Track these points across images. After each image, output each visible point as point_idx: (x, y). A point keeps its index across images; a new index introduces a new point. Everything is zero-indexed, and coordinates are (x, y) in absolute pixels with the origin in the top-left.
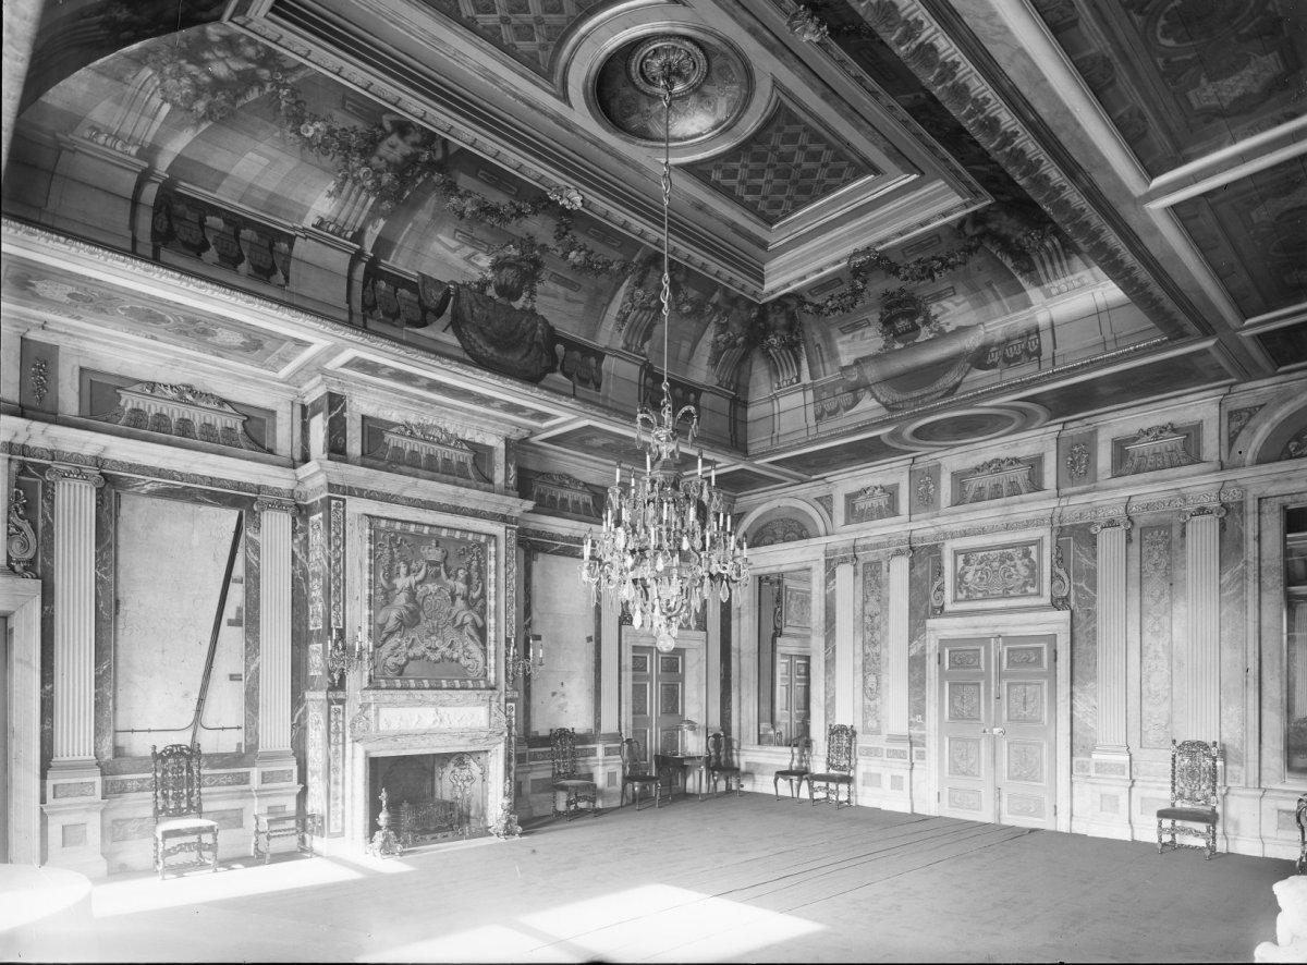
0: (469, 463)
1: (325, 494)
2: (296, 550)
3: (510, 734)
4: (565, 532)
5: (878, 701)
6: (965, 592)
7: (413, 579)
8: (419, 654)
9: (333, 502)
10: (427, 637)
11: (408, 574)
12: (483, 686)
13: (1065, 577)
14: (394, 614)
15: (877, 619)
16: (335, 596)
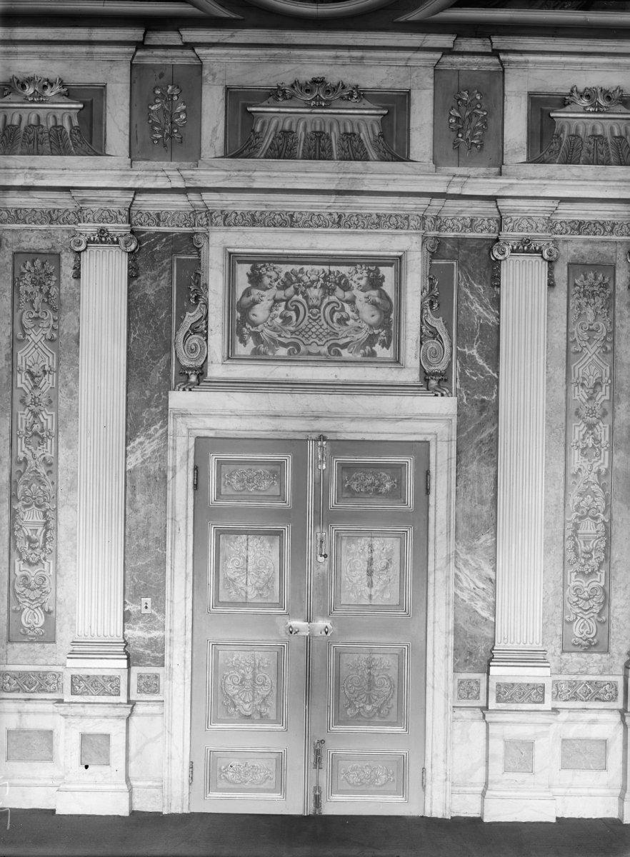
5: (48, 568)
13: (444, 336)
15: (47, 382)
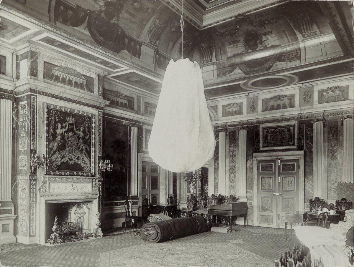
0: (85, 84)
1: (29, 93)
2: (14, 116)
3: (100, 195)
4: (118, 115)
6: (267, 143)
7: (63, 130)
9: (32, 97)
10: (68, 154)
11: (61, 128)
12: (90, 175)
13: (302, 139)
14: (56, 144)
16: (33, 136)
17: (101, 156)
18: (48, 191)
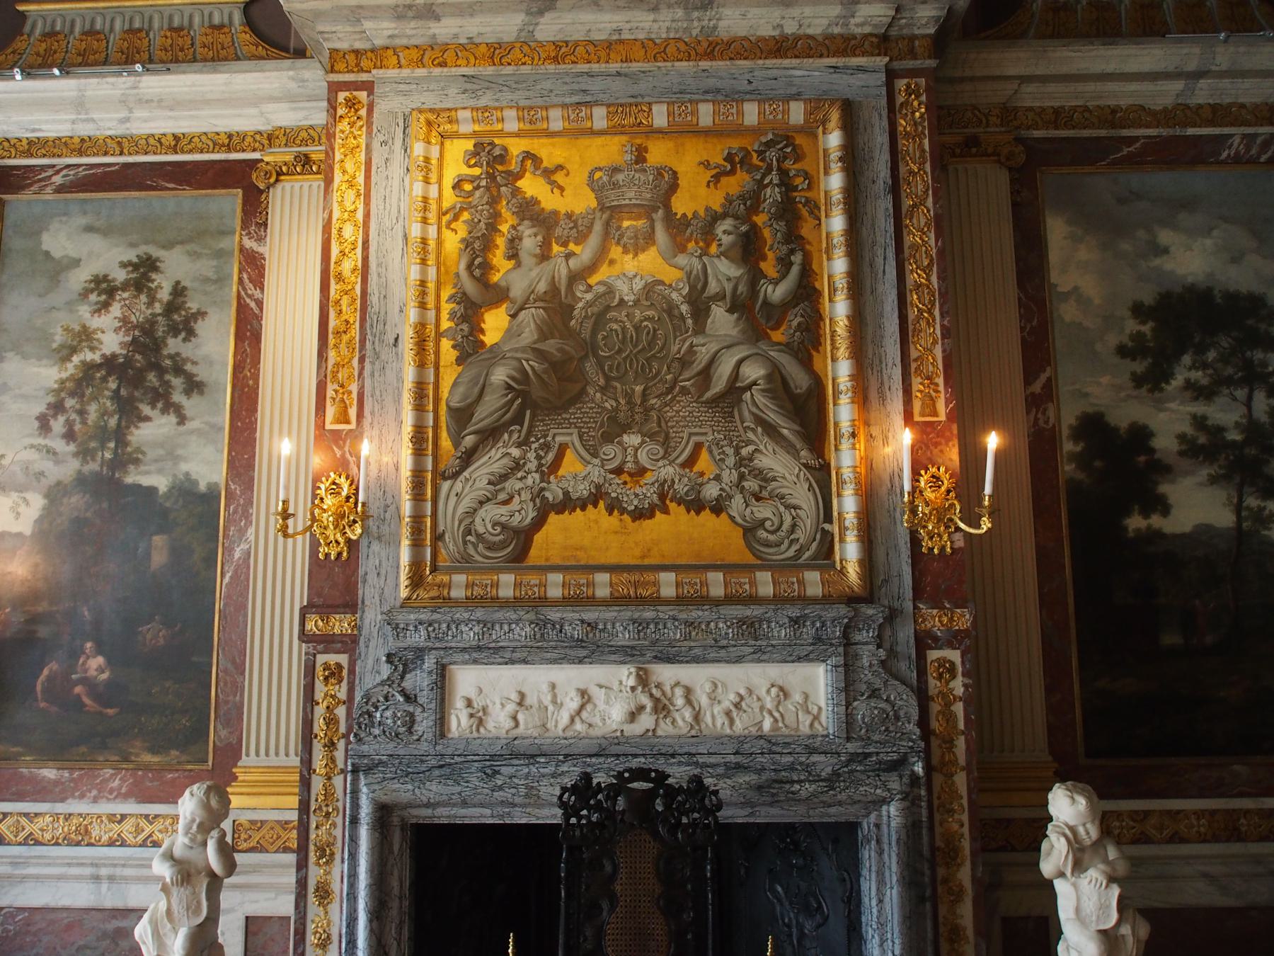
8: (582, 490)
17: (942, 417)
18: (424, 724)
